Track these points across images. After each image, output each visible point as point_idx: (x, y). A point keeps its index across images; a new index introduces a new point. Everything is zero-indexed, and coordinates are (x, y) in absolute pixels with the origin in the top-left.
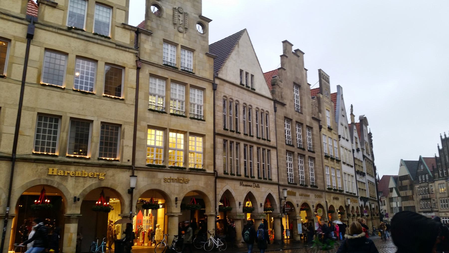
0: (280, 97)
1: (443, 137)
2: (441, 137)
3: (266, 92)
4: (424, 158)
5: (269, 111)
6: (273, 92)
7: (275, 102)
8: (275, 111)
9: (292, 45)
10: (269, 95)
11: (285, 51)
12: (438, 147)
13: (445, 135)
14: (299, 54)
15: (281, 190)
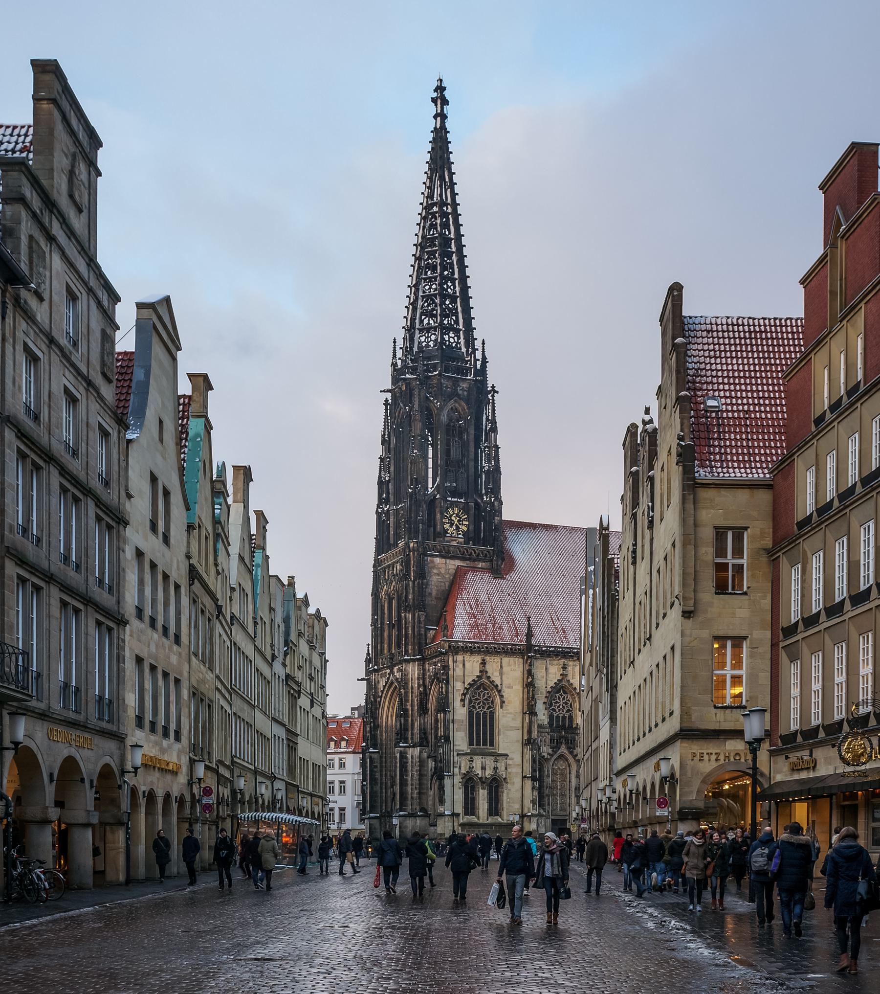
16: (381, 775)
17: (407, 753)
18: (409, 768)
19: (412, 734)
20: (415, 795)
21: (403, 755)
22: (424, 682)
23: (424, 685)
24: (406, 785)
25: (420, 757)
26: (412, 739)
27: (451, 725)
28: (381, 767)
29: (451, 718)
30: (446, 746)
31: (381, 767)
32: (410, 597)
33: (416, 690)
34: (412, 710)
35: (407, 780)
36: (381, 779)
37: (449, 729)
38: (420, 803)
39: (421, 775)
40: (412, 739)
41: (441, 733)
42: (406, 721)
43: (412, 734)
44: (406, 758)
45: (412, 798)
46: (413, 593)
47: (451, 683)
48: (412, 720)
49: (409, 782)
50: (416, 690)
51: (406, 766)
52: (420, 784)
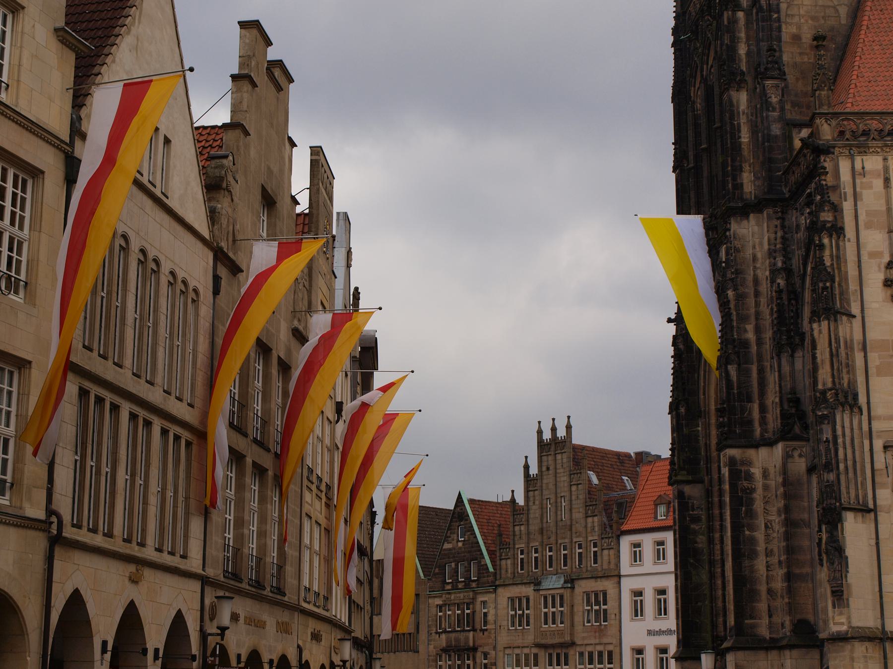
0: (231, 239)
1: (547, 435)
2: (540, 432)
3: (195, 212)
4: (472, 502)
5: (201, 290)
6: (213, 216)
7: (220, 256)
8: (216, 291)
9: (269, 43)
10: (201, 225)
11: (245, 60)
12: (526, 467)
13: (554, 429)
14: (277, 73)
15: (207, 602)
16: (711, 541)
17: (749, 463)
18: (758, 506)
19: (763, 409)
20: (779, 585)
21: (739, 472)
22: (787, 258)
23: (788, 271)
24: (753, 554)
25: (784, 471)
26: (763, 421)
27: (859, 357)
28: (710, 518)
29: (857, 336)
30: (843, 419)
31: (710, 518)
32: (742, 50)
33: (764, 287)
34: (760, 342)
35: (753, 541)
36: (711, 553)
37: (850, 367)
38: (792, 608)
39: (791, 524)
40: (763, 421)
41: (825, 376)
42: (744, 373)
43: (763, 409)
44: (749, 477)
45: (770, 591)
46: (748, 38)
47: (850, 232)
48: (761, 371)
49: (761, 547)
50: (764, 287)
51: (751, 501)
52: (790, 550)
